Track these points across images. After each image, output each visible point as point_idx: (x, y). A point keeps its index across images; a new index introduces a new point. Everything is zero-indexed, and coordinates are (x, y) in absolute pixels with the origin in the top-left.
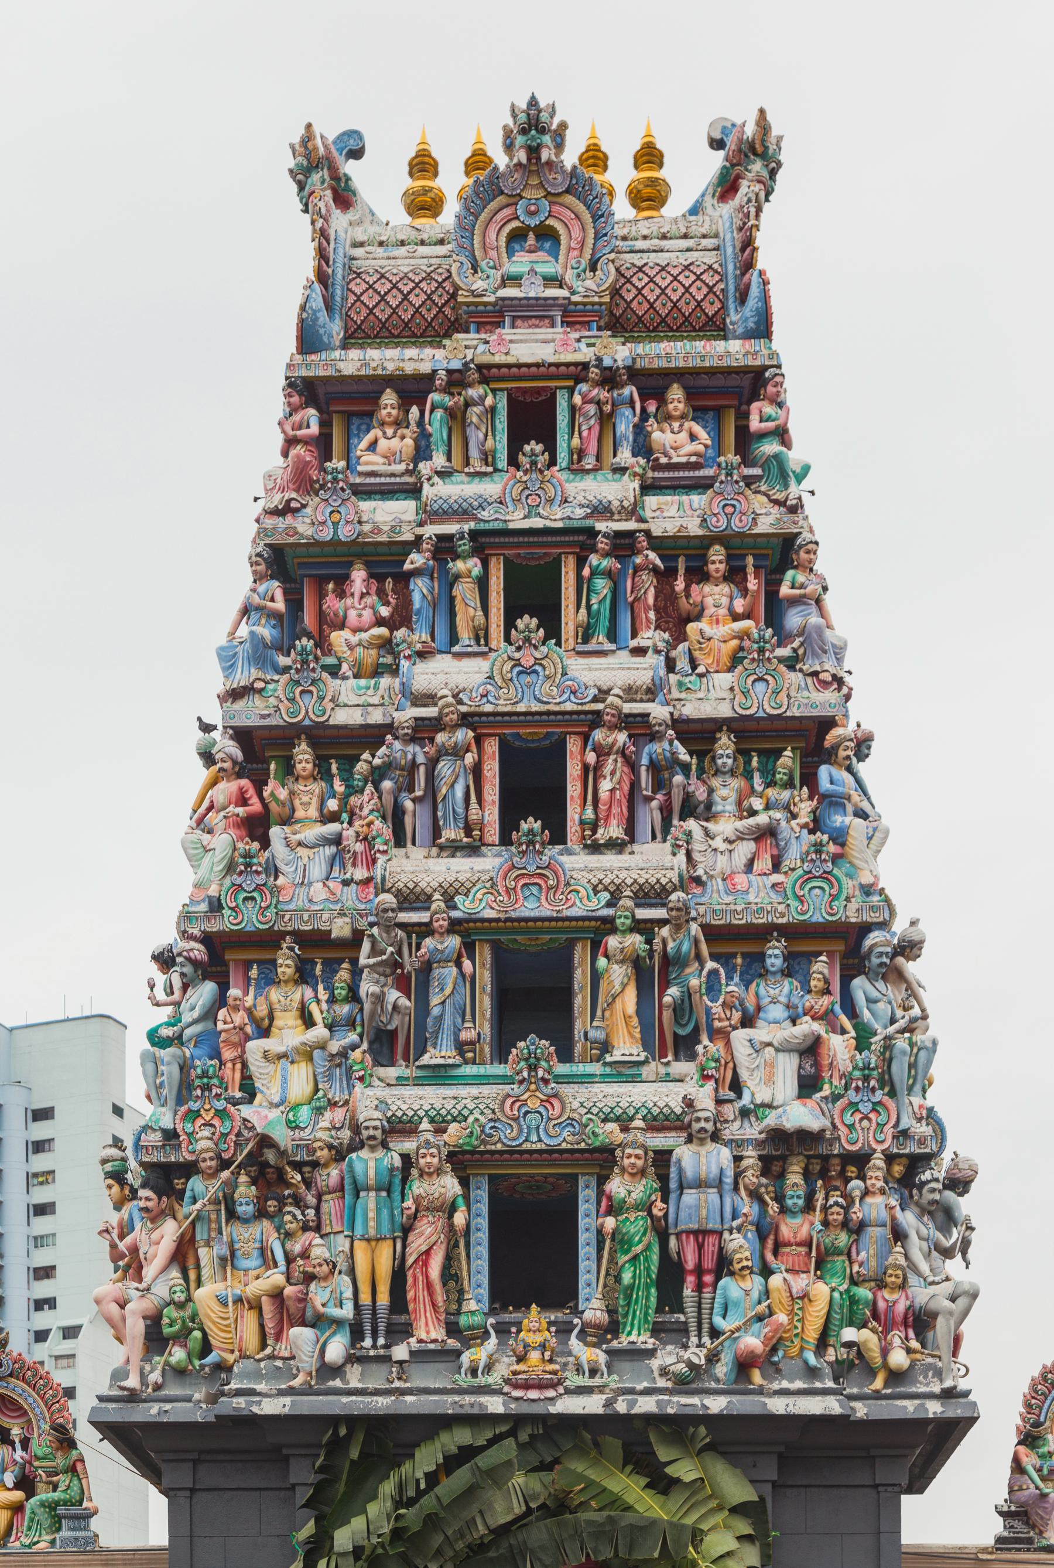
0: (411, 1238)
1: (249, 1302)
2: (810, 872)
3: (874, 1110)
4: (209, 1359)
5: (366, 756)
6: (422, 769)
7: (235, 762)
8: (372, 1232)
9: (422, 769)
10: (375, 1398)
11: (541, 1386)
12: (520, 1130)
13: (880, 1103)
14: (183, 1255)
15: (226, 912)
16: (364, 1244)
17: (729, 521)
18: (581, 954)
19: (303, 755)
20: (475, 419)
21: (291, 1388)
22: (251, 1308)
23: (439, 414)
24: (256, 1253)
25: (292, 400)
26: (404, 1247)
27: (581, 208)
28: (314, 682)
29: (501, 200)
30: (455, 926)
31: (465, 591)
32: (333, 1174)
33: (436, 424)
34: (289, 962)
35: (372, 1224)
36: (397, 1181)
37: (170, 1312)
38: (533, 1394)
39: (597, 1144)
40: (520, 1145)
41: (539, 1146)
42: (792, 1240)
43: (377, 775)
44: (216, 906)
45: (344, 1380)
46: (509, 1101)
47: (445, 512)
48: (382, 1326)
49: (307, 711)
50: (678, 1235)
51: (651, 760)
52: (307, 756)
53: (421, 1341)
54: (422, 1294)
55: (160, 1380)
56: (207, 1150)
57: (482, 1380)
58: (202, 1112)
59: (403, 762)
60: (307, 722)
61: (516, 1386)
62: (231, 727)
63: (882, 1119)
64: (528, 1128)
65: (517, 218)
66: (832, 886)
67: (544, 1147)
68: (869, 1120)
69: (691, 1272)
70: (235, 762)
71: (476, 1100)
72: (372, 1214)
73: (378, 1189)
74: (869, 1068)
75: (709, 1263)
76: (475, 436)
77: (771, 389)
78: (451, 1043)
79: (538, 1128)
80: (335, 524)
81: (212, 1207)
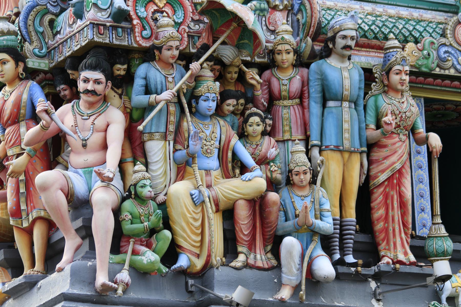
0: (377, 154)
4: (183, 261)
16: (337, 156)
35: (346, 135)
48: (350, 244)
56: (171, 38)
73: (350, 101)
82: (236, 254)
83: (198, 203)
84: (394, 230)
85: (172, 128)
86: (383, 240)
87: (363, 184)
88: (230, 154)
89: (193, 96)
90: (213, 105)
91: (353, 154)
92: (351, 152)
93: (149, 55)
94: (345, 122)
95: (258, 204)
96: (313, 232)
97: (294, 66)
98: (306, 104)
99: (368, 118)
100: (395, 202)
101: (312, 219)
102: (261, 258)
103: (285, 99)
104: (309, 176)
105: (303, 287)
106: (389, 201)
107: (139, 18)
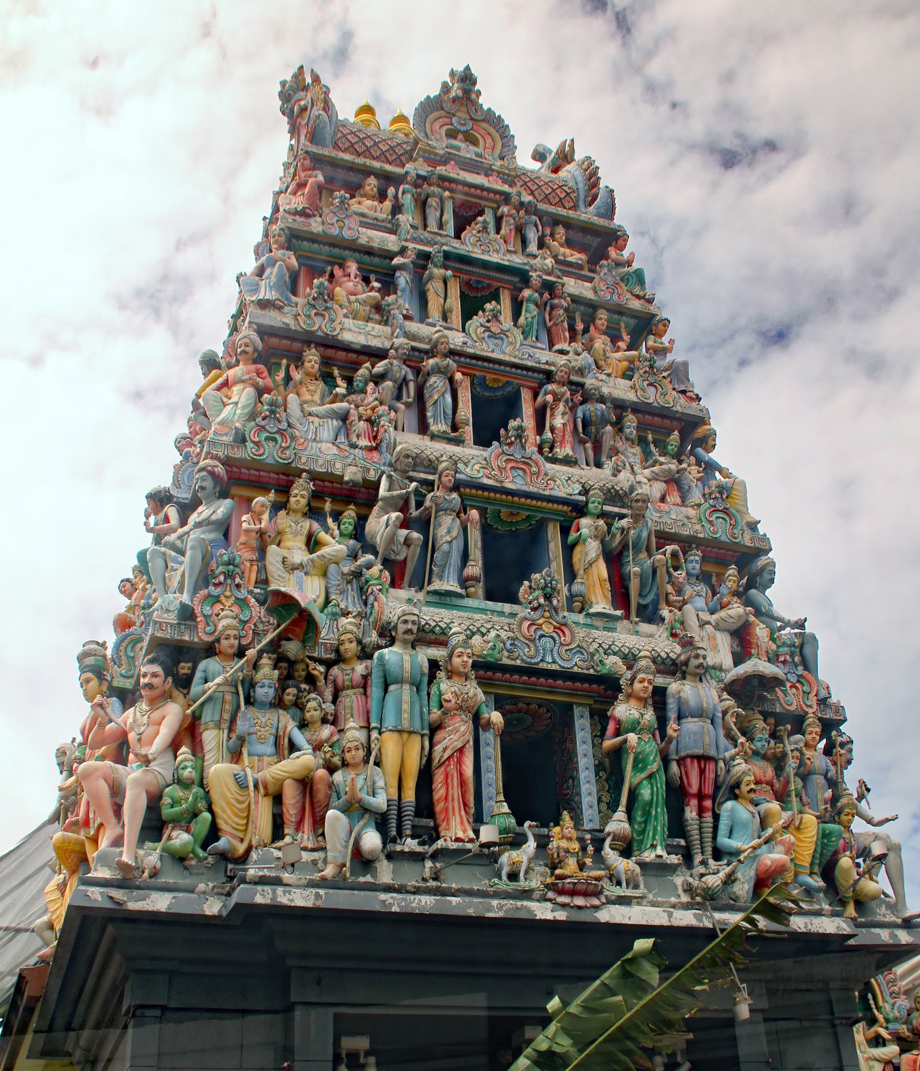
0: (439, 736)
1: (265, 788)
2: (715, 506)
3: (798, 681)
4: (222, 843)
5: (368, 365)
6: (412, 385)
7: (255, 350)
8: (406, 725)
9: (412, 385)
10: (417, 897)
11: (586, 894)
12: (537, 651)
13: (801, 676)
14: (189, 732)
15: (249, 444)
16: (395, 736)
17: (612, 297)
18: (553, 533)
19: (312, 358)
20: (434, 204)
21: (324, 879)
22: (266, 795)
23: (409, 196)
24: (272, 739)
25: (306, 162)
26: (432, 746)
27: (492, 131)
28: (326, 309)
29: (442, 113)
30: (456, 487)
31: (434, 289)
32: (360, 668)
33: (407, 200)
34: (304, 493)
36: (426, 680)
37: (174, 791)
38: (579, 901)
39: (605, 671)
40: (537, 663)
41: (554, 667)
42: (763, 779)
43: (378, 379)
44: (241, 439)
45: (374, 876)
46: (527, 623)
47: (422, 240)
49: (320, 326)
50: (681, 762)
51: (584, 415)
52: (316, 358)
53: (458, 840)
54: (455, 791)
55: (159, 865)
57: (523, 884)
58: (222, 598)
59: (398, 375)
60: (320, 333)
61: (561, 892)
62: (257, 324)
63: (806, 688)
64: (544, 649)
65: (452, 124)
66: (731, 519)
67: (558, 668)
68: (797, 688)
69: (694, 796)
70: (255, 350)
71: (483, 627)
72: (406, 706)
74: (794, 646)
75: (709, 789)
76: (433, 216)
77: (620, 242)
78: (456, 577)
79: (552, 650)
80: (341, 228)
81: (227, 688)
82: (282, 837)
83: (242, 784)
84: (453, 808)
85: (227, 716)
86: (443, 821)
87: (424, 766)
88: (286, 741)
89: (250, 684)
90: (271, 692)
91: (413, 735)
92: (410, 733)
93: (210, 650)
94: (402, 703)
95: (305, 783)
96: (365, 810)
97: (359, 658)
98: (368, 693)
99: (431, 704)
100: (455, 780)
101: (363, 795)
102: (306, 837)
103: (348, 689)
104: (361, 753)
105: (348, 864)
106: (449, 780)
107: (204, 616)
